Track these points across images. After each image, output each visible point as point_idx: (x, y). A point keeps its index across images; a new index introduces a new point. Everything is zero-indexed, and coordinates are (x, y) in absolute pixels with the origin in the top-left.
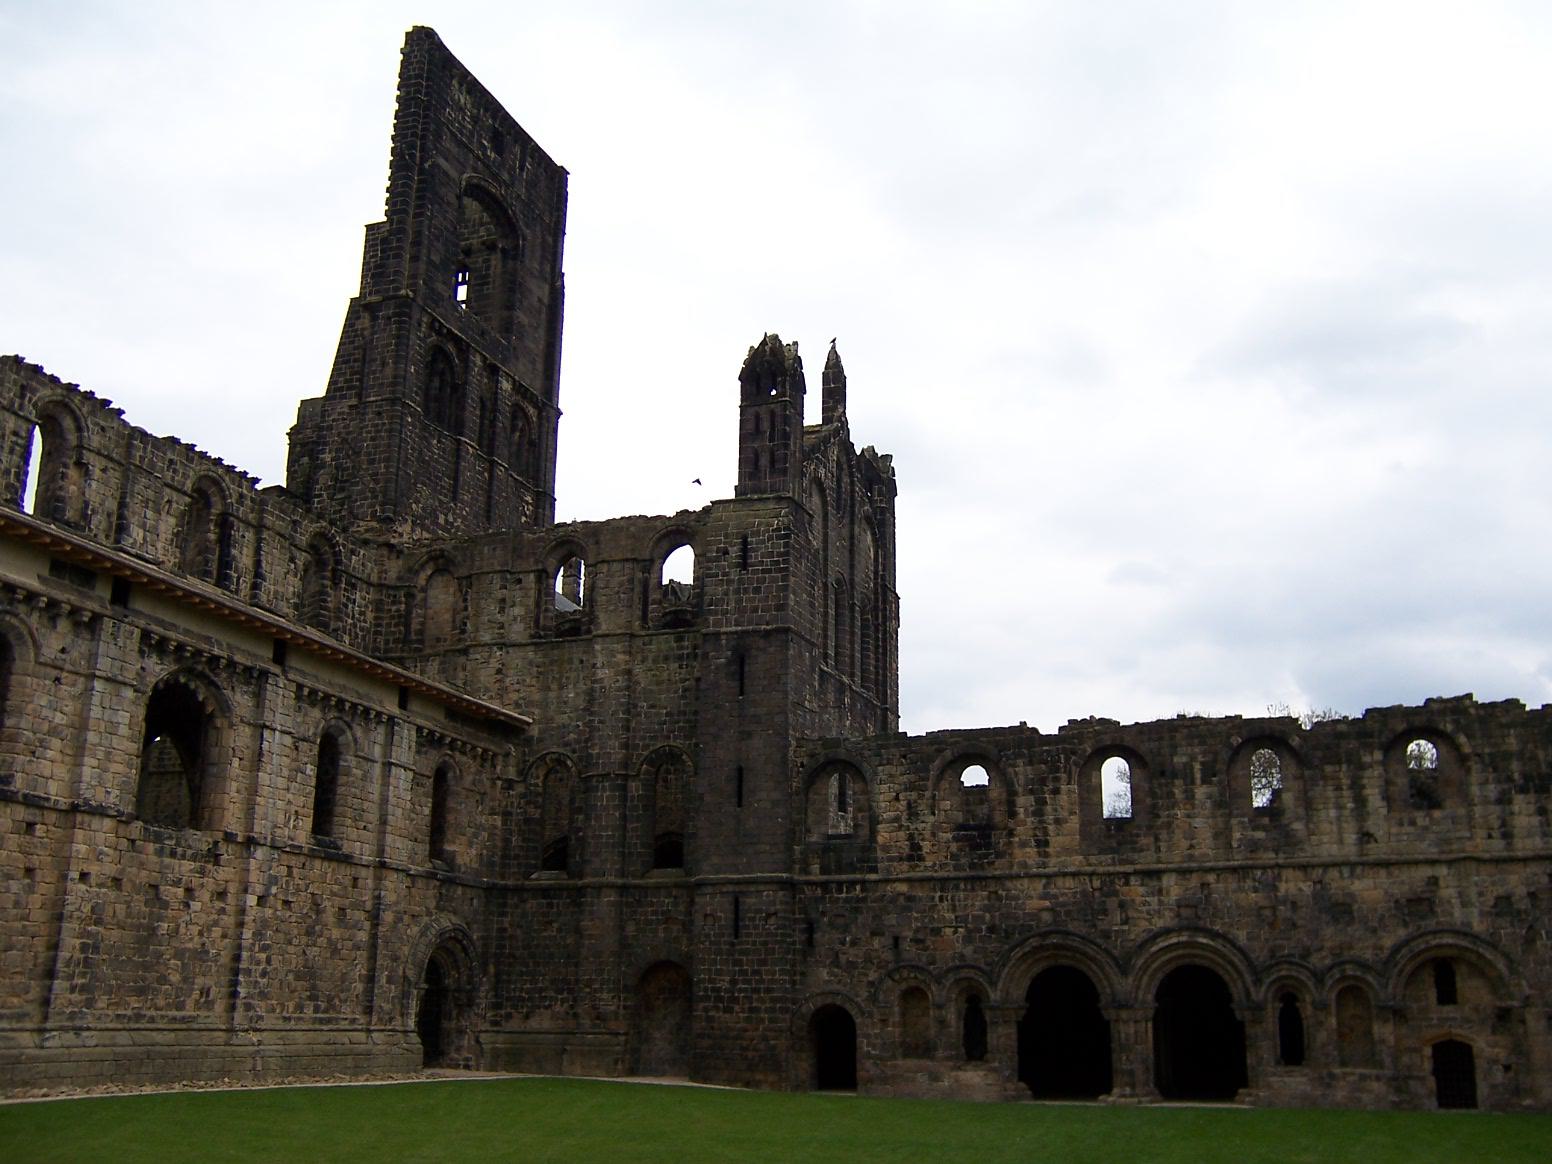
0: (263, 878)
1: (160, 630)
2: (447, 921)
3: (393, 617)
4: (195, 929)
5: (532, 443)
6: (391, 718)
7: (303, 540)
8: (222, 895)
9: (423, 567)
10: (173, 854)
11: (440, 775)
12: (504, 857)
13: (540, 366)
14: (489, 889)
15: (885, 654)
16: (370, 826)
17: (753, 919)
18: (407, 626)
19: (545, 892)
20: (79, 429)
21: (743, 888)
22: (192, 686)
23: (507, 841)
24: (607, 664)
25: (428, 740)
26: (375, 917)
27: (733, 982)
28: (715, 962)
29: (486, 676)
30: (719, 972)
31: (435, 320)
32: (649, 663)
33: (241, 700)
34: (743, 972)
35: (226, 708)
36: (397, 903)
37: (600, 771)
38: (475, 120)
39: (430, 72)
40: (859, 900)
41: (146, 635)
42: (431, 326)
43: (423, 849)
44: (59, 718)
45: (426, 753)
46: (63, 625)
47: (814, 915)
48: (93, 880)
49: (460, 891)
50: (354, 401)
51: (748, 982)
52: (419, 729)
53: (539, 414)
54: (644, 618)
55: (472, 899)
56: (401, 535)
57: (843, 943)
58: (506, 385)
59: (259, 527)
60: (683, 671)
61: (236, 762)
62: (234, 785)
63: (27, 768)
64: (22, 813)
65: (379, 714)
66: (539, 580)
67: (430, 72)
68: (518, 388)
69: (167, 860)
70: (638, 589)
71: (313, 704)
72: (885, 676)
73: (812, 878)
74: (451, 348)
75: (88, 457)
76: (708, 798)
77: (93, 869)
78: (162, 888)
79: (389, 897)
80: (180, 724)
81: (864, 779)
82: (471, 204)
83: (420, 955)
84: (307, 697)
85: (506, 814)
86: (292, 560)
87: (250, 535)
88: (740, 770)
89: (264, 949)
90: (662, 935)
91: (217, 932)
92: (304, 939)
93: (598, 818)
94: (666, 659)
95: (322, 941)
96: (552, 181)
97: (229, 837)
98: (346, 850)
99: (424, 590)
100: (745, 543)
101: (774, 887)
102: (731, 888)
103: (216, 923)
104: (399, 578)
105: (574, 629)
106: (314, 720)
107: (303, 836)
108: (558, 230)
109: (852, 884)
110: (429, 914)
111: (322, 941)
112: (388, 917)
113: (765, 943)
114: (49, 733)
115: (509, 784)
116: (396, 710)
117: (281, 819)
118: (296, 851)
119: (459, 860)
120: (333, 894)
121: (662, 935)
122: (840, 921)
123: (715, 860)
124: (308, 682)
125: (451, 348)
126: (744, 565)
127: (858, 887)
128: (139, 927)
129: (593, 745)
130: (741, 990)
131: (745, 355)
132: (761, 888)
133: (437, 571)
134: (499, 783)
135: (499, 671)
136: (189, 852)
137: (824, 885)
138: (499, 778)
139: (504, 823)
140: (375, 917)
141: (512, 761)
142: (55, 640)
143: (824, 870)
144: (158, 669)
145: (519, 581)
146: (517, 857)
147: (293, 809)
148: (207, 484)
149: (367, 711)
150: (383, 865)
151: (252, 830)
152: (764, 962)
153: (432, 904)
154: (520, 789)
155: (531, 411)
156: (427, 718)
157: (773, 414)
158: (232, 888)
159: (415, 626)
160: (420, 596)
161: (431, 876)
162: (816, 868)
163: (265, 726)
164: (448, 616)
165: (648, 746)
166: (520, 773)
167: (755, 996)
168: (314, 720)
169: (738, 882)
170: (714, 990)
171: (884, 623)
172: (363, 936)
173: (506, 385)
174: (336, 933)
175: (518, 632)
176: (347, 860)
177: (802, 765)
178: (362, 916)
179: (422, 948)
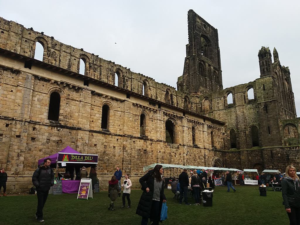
0: (186, 151)
1: (166, 112)
2: (216, 158)
3: (199, 108)
4: (177, 160)
5: (218, 77)
6: (203, 124)
7: (183, 97)
8: (180, 154)
9: (203, 99)
10: (172, 148)
11: (212, 133)
13: (217, 64)
14: (222, 152)
15: (292, 104)
16: (202, 142)
18: (202, 109)
19: (232, 152)
20: (149, 83)
21: (273, 149)
22: (171, 120)
23: (224, 143)
24: (239, 111)
25: (209, 127)
26: (205, 158)
28: (268, 163)
29: (217, 116)
31: (199, 58)
32: (247, 110)
33: (179, 122)
35: (177, 124)
36: (208, 155)
37: (240, 130)
38: (201, 24)
39: (192, 16)
40: (298, 150)
41: (164, 112)
42: (199, 60)
43: (211, 146)
44: (153, 127)
46: (152, 112)
47: (288, 153)
48: (161, 152)
49: (218, 152)
50: (188, 74)
52: (208, 125)
53: (218, 72)
54: (245, 102)
56: (199, 95)
57: (296, 159)
58: (212, 68)
59: (177, 96)
61: (180, 132)
62: (180, 136)
63: (150, 135)
64: (150, 142)
65: (201, 123)
66: (224, 98)
67: (192, 16)
68: (214, 68)
69: (171, 149)
70: (243, 97)
71: (190, 122)
72: (293, 108)
73: (287, 146)
74: (202, 63)
75: (151, 88)
76: (263, 133)
77: (161, 150)
78: (171, 153)
79: (207, 154)
80: (170, 128)
81: (296, 127)
82: (203, 40)
83: (213, 164)
84: (190, 121)
85: (224, 139)
86: (182, 100)
87: (175, 97)
88: (269, 127)
89: (188, 163)
91: (180, 160)
92: (194, 161)
93: (241, 138)
94: (250, 109)
95: (197, 162)
96: (215, 32)
97: (180, 145)
98: (198, 146)
99: (204, 103)
100: (264, 85)
101: (279, 148)
102: (270, 149)
103: (180, 159)
104: (199, 102)
105: (230, 106)
106: (191, 125)
107: (191, 144)
108: (217, 40)
109: (296, 147)
110: (213, 157)
111: (197, 162)
112: (207, 157)
114: (152, 129)
115: (224, 134)
116: (203, 122)
117: (188, 141)
118: (191, 146)
119: (217, 147)
120: (197, 154)
121: (256, 159)
122: (294, 154)
124: (189, 118)
125: (202, 63)
126: (264, 90)
127: (297, 148)
128: (169, 160)
131: (258, 52)
132: (276, 149)
133: (206, 100)
135: (219, 115)
136: (175, 147)
137: (290, 148)
138: (222, 133)
139: (224, 140)
140: (205, 158)
141: (223, 130)
142: (151, 114)
143: (290, 145)
144: (166, 118)
145: (221, 99)
146: (227, 146)
147: (189, 140)
148: (168, 89)
149: (199, 122)
150: (205, 148)
151: (184, 143)
154: (226, 134)
155: (217, 72)
156: (208, 123)
157: (266, 61)
158: (182, 153)
159: (203, 109)
160: (203, 104)
161: (212, 150)
162: (287, 145)
163: (183, 126)
164: (208, 107)
165: (249, 125)
166: (225, 132)
168: (191, 125)
171: (291, 98)
172: (203, 161)
173: (212, 68)
174: (199, 160)
175: (221, 107)
176: (199, 148)
177: (282, 125)
178: (202, 157)
179: (213, 163)
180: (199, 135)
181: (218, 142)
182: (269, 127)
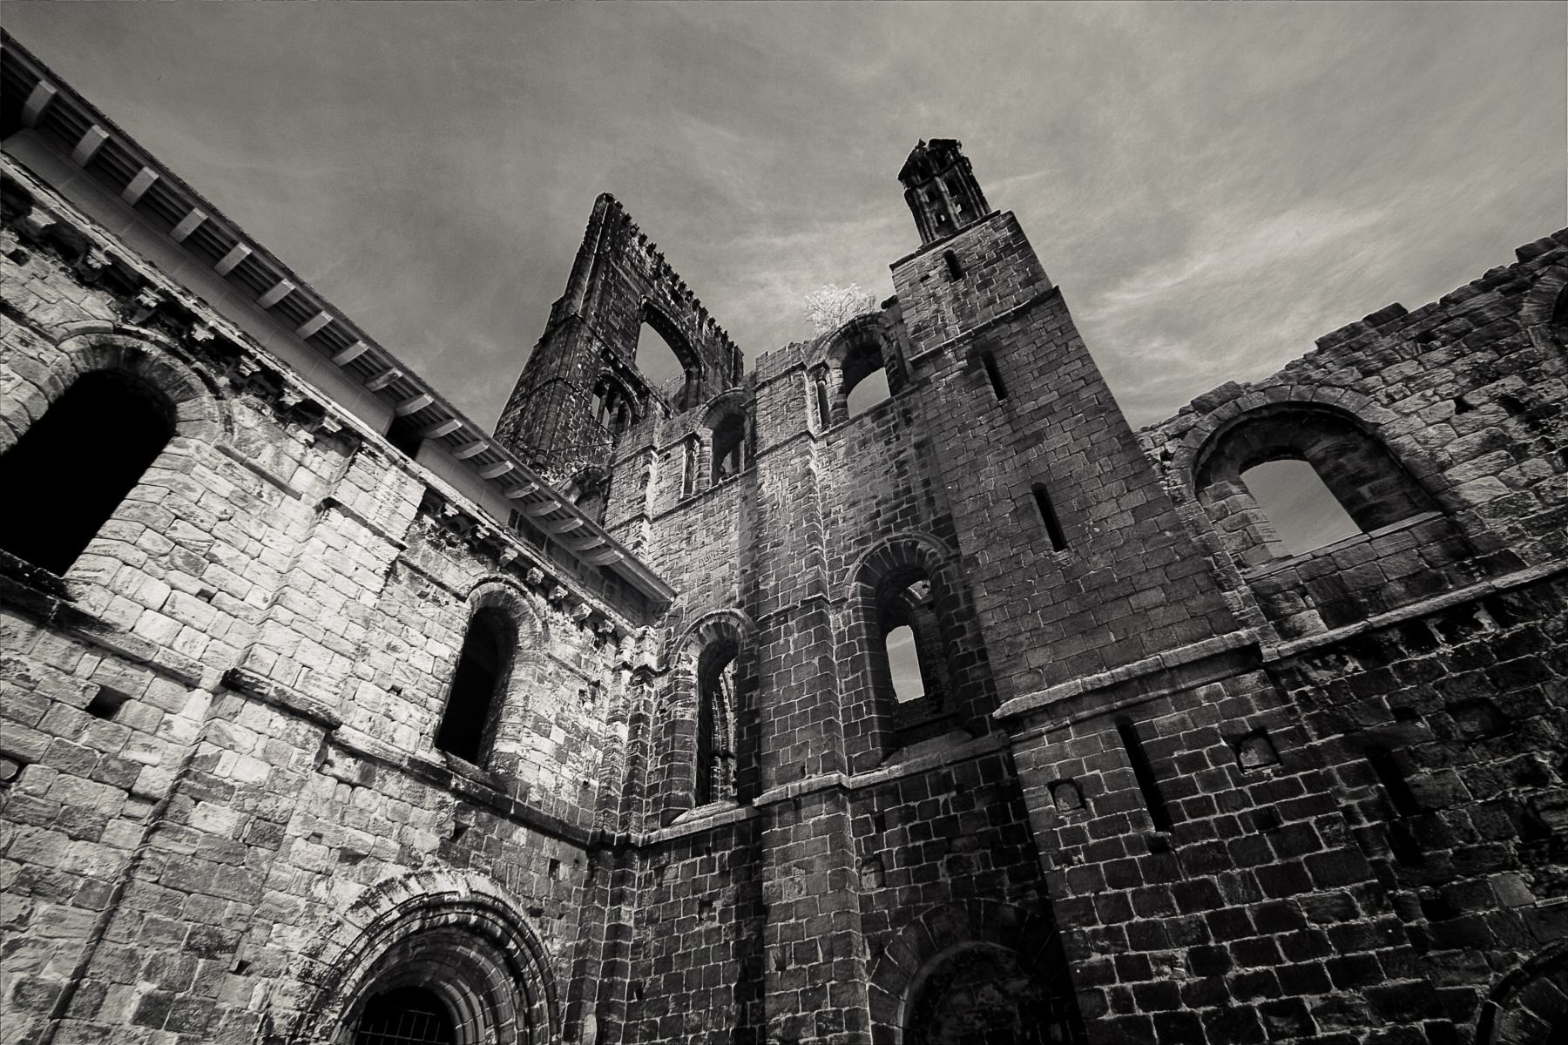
2: (451, 883)
12: (629, 790)
14: (597, 846)
17: (1194, 763)
27: (1204, 961)
28: (1118, 908)
30: (1149, 936)
34: (1229, 924)
36: (257, 790)
45: (458, 556)
49: (521, 835)
51: (1264, 953)
52: (432, 501)
55: (554, 864)
60: (892, 446)
76: (985, 558)
85: (637, 719)
88: (1042, 496)
90: (946, 879)
98: (90, 601)
113: (1267, 821)
115: (645, 674)
119: (527, 774)
121: (946, 879)
123: (1038, 658)
129: (767, 577)
130: (1245, 987)
134: (626, 674)
138: (626, 666)
139: (633, 733)
152: (1289, 880)
153: (426, 841)
166: (664, 660)
167: (1310, 1001)
169: (1117, 687)
170: (1150, 997)
179: (348, 935)
180: (218, 507)
181: (558, 736)
182: (1042, 496)
